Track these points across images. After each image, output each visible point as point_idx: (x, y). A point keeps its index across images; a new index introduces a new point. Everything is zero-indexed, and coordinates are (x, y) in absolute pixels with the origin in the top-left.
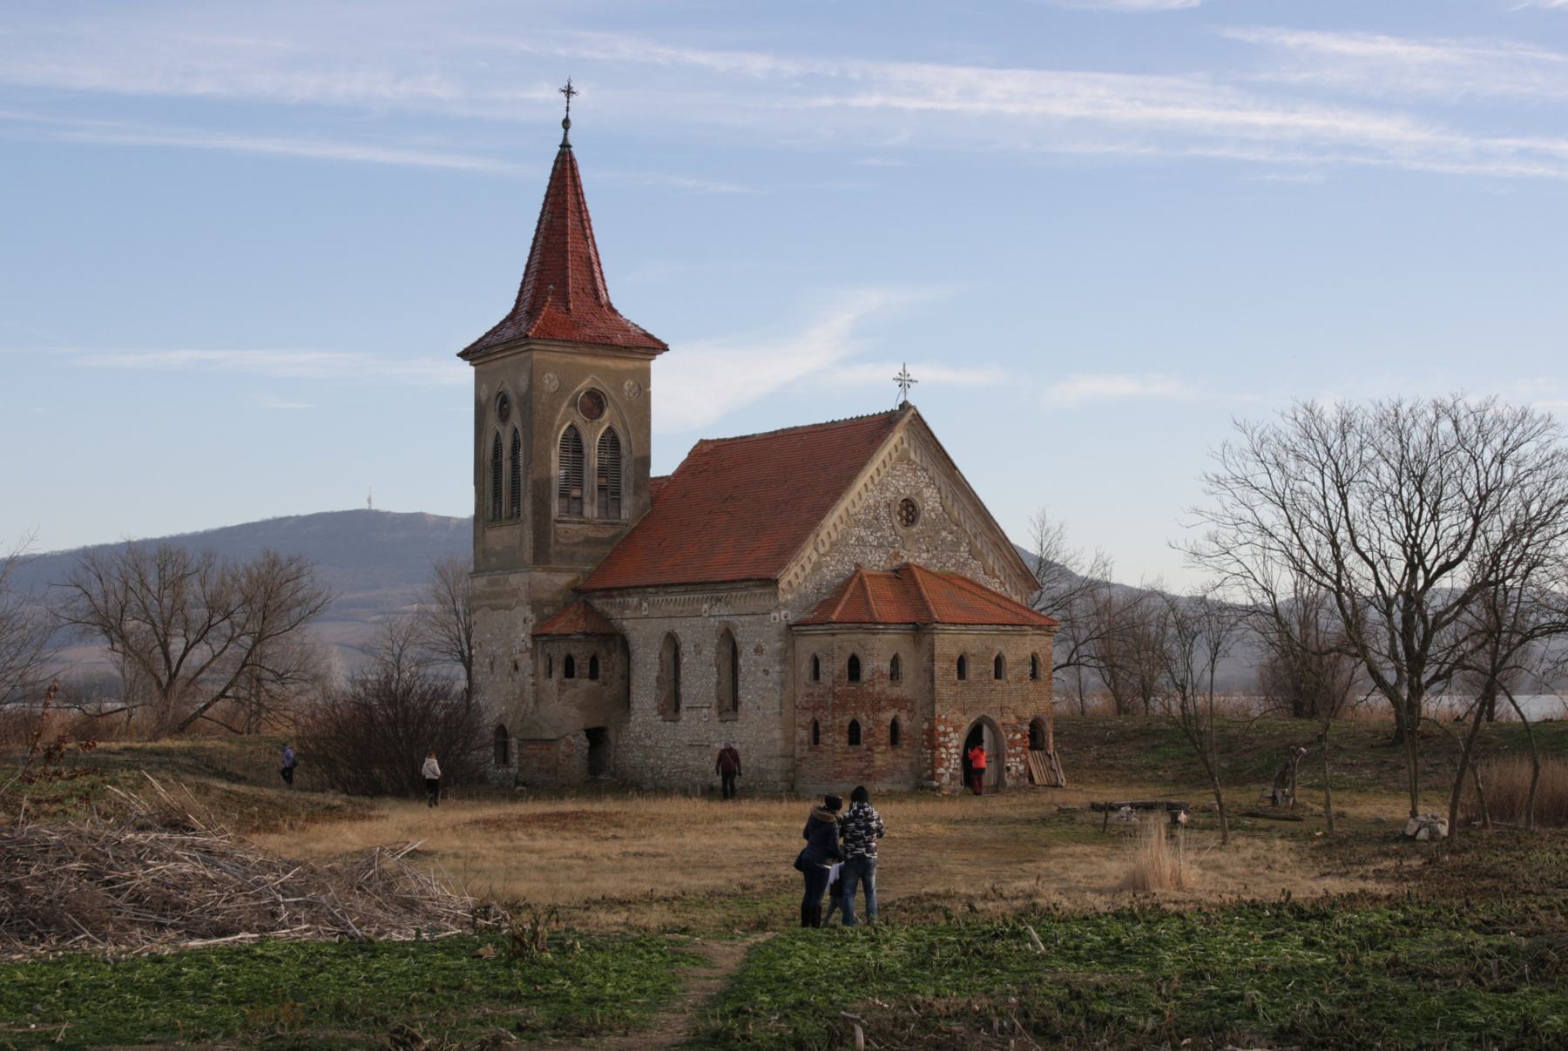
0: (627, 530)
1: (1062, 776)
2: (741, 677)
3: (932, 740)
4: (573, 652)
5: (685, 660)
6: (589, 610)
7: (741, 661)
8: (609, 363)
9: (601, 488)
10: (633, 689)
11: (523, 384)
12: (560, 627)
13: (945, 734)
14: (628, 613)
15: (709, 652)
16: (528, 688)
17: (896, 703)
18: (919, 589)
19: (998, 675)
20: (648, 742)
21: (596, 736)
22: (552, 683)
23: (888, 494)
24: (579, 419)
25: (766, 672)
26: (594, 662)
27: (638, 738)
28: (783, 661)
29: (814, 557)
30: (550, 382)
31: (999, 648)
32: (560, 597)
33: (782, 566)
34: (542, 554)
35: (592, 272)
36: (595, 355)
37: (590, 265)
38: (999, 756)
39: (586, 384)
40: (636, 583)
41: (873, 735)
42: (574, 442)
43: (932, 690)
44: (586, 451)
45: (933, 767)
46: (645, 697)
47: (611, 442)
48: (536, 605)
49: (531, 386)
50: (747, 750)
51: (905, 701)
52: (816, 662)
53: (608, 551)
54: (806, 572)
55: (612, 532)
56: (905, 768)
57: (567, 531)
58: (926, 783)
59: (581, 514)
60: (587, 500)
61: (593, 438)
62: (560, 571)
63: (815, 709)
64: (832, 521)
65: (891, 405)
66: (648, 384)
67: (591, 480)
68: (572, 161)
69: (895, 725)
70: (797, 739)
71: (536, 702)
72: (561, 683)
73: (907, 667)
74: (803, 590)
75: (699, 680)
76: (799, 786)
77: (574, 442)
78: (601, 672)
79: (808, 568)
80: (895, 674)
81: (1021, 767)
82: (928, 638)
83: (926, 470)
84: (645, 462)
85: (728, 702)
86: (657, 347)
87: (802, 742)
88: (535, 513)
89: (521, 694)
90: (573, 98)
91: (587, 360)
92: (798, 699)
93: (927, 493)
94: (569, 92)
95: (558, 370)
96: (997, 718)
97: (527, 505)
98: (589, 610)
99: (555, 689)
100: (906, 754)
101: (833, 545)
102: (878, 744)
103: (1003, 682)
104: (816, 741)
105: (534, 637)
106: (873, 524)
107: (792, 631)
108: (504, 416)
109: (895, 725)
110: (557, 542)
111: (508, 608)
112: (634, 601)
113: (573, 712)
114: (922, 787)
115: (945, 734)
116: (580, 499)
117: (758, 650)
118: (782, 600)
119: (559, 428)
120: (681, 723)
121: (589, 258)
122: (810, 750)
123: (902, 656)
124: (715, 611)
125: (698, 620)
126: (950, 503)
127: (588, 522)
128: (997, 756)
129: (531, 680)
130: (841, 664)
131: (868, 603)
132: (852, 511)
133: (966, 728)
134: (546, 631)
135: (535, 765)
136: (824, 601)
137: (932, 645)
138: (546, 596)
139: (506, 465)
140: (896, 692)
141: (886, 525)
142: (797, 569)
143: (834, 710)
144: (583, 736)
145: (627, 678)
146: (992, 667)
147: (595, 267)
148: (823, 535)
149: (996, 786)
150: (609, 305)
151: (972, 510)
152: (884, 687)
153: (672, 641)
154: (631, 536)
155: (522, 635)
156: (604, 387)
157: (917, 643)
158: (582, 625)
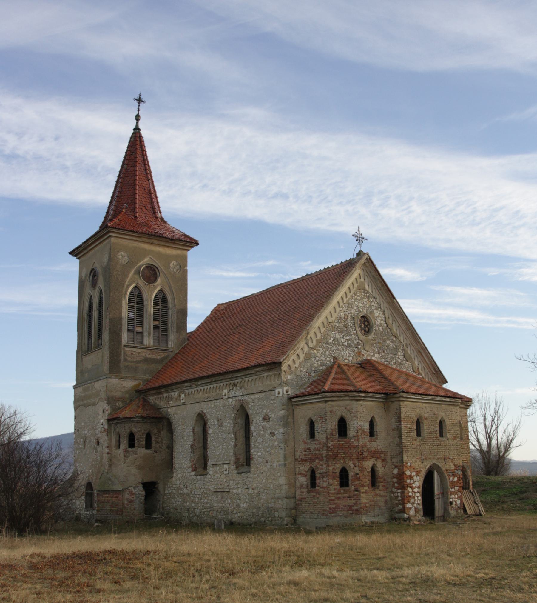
0: (172, 355)
1: (481, 508)
2: (252, 440)
3: (401, 481)
4: (134, 430)
5: (211, 431)
6: (146, 404)
7: (252, 428)
8: (161, 250)
9: (155, 327)
10: (175, 454)
11: (105, 259)
12: (126, 413)
13: (411, 477)
14: (172, 403)
15: (228, 424)
16: (106, 456)
17: (374, 454)
18: (381, 373)
20: (185, 491)
21: (150, 488)
22: (121, 451)
23: (353, 311)
24: (141, 283)
25: (273, 434)
26: (148, 438)
27: (179, 489)
28: (285, 425)
30: (122, 257)
31: (442, 414)
32: (127, 396)
33: (284, 353)
34: (115, 366)
35: (152, 198)
36: (152, 244)
37: (151, 195)
38: (444, 493)
39: (146, 260)
40: (174, 381)
41: (359, 479)
42: (137, 299)
43: (401, 443)
44: (145, 303)
45: (403, 504)
46: (183, 459)
47: (161, 300)
48: (111, 400)
49: (110, 259)
50: (258, 493)
51: (380, 452)
52: (312, 424)
53: (160, 368)
54: (301, 360)
55: (163, 355)
56: (382, 504)
57: (132, 353)
58: (397, 516)
59: (142, 343)
60: (146, 334)
61: (150, 295)
62: (126, 378)
63: (312, 460)
64: (318, 322)
65: (351, 255)
66: (186, 265)
67: (149, 321)
68: (141, 137)
69: (373, 471)
70: (298, 484)
71: (110, 466)
72: (126, 451)
73: (380, 427)
74: (298, 373)
75: (222, 444)
76: (300, 520)
77: (137, 299)
78: (154, 444)
79: (302, 357)
80: (372, 433)
81: (459, 502)
82: (394, 406)
83: (375, 298)
84: (183, 313)
85: (242, 459)
86: (190, 243)
87: (302, 486)
88: (111, 340)
89: (101, 461)
90: (142, 105)
91: (147, 246)
92: (298, 454)
93: (377, 313)
94: (139, 101)
95: (125, 248)
97: (106, 336)
98: (146, 404)
99: (122, 455)
100: (382, 493)
101: (318, 342)
102: (363, 486)
103: (444, 439)
104: (313, 483)
105: (109, 420)
106: (344, 330)
107: (292, 401)
108: (94, 284)
109: (373, 471)
110: (125, 360)
111: (94, 404)
112: (175, 394)
113: (134, 471)
114: (395, 519)
115: (411, 477)
116: (141, 333)
117: (266, 418)
118: (284, 377)
120: (208, 476)
121: (150, 190)
122: (308, 492)
123: (377, 418)
124: (232, 394)
125: (218, 404)
126: (390, 322)
127: (147, 348)
128: (443, 493)
129: (107, 450)
130: (333, 425)
131: (349, 379)
132: (330, 320)
133: (423, 473)
134: (116, 416)
135: (108, 508)
136: (314, 382)
137: (399, 410)
138: (118, 394)
139: (95, 314)
140: (373, 445)
141: (352, 332)
142: (294, 357)
143: (328, 460)
144: (141, 487)
145: (170, 448)
146: (438, 428)
147: (154, 200)
148: (311, 334)
149: (443, 516)
150: (162, 219)
151: (404, 327)
152: (365, 441)
153: (202, 419)
154: (174, 358)
155: (102, 420)
156: (157, 263)
157: (387, 409)
158: (140, 412)
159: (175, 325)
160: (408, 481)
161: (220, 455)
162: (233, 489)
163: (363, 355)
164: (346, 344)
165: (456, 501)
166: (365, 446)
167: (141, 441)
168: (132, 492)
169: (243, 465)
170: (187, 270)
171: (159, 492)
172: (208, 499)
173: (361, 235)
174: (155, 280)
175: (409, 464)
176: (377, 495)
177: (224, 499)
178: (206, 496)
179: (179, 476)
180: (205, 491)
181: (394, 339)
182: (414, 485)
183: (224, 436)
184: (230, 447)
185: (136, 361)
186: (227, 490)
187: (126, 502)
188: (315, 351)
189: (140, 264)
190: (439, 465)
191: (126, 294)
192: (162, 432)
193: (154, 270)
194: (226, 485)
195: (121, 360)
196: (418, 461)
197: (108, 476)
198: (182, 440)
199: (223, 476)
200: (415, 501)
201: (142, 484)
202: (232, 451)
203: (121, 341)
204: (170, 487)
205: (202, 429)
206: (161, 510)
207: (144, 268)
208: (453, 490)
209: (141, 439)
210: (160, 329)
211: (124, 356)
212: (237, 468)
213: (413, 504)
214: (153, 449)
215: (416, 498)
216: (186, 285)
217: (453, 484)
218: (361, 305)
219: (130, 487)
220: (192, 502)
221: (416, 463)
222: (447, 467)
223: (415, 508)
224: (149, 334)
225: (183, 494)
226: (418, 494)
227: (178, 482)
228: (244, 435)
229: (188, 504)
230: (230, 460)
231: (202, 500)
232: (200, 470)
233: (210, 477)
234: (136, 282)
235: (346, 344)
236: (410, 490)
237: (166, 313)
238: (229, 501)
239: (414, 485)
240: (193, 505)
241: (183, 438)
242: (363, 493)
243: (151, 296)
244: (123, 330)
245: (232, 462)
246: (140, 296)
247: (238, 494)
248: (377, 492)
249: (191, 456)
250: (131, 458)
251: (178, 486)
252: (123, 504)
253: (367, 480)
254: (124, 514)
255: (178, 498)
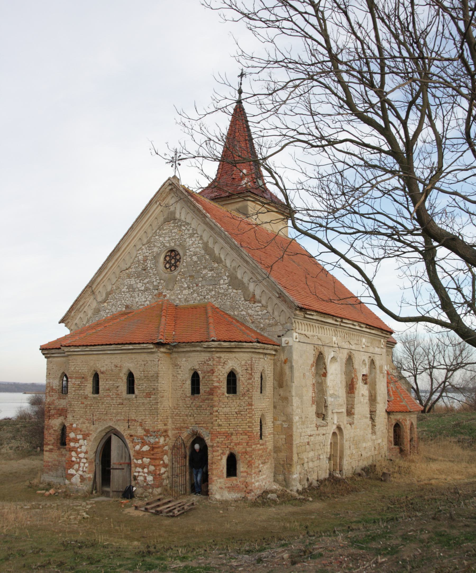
13: (76, 440)
19: (131, 390)
23: (155, 249)
29: (94, 305)
79: (90, 313)
96: (120, 428)
101: (108, 294)
115: (76, 440)
160: (72, 444)
163: (165, 296)
164: (143, 288)
165: (145, 477)
166: (53, 403)
173: (172, 158)
175: (74, 425)
176: (63, 455)
181: (216, 265)
182: (79, 450)
188: (106, 304)
190: (118, 428)
196: (87, 422)
200: (79, 467)
208: (140, 462)
213: (77, 470)
215: (82, 465)
217: (140, 455)
218: (167, 239)
221: (84, 425)
222: (132, 432)
223: (81, 476)
226: (84, 461)
235: (143, 288)
236: (73, 454)
239: (79, 450)
242: (46, 451)
248: (63, 452)
253: (51, 438)
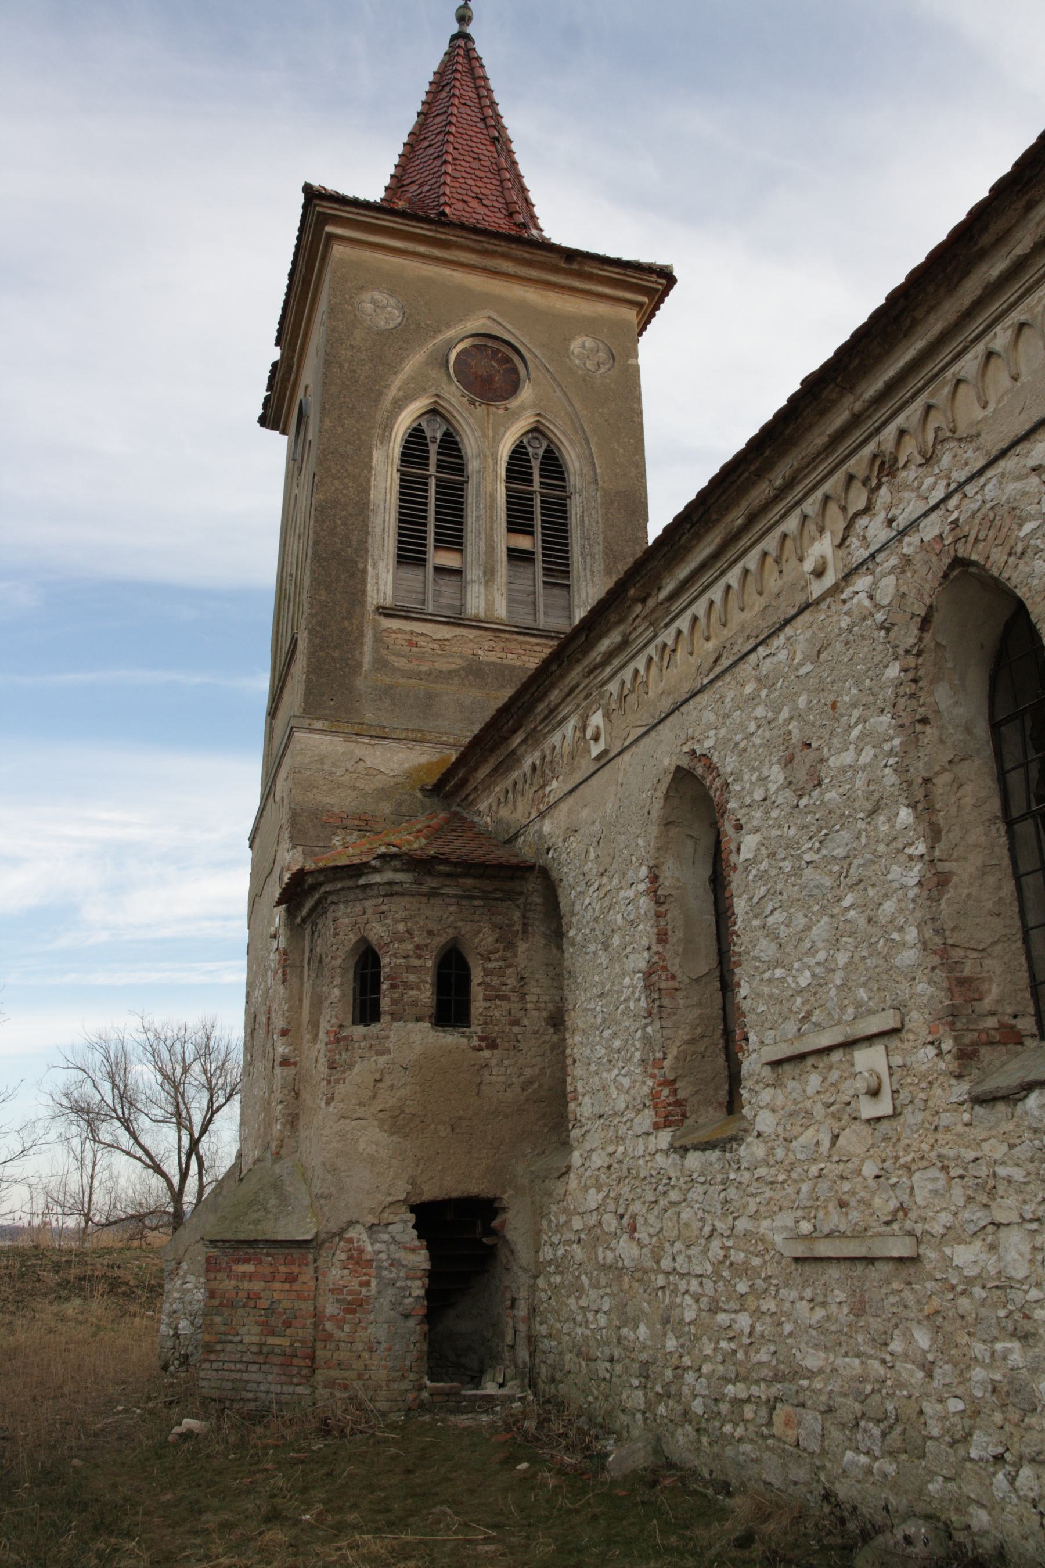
4: (377, 932)
8: (532, 295)
9: (516, 556)
20: (627, 1250)
24: (454, 396)
27: (595, 1237)
44: (473, 466)
46: (612, 1071)
60: (474, 574)
61: (490, 448)
72: (338, 1040)
78: (478, 1004)
86: (648, 286)
110: (381, 664)
113: (372, 1139)
119: (399, 405)
120: (752, 1150)
135: (251, 1335)
159: (598, 550)
161: (819, 983)
162: (951, 1235)
167: (408, 986)
168: (361, 1251)
169: (1011, 1037)
170: (636, 369)
171: (512, 1252)
172: (758, 1314)
174: (513, 388)
177: (876, 1324)
178: (742, 1287)
179: (598, 1160)
180: (738, 1257)
183: (840, 844)
184: (889, 907)
185: (429, 674)
186: (900, 1248)
187: (331, 1309)
189: (451, 333)
191: (388, 426)
192: (522, 946)
193: (508, 360)
194: (884, 1204)
195: (360, 665)
197: (277, 1168)
198: (603, 959)
199: (853, 1140)
201: (413, 1209)
202: (912, 934)
203: (364, 593)
204: (559, 1229)
205: (706, 873)
206: (523, 1354)
207: (464, 351)
209: (412, 978)
210: (539, 565)
211: (375, 650)
212: (966, 1055)
214: (476, 1028)
216: (640, 414)
219: (351, 1223)
220: (666, 1321)
224: (490, 574)
225: (615, 1269)
227: (594, 1198)
228: (995, 805)
229: (643, 1330)
230: (898, 1008)
231: (722, 1318)
232: (708, 1120)
233: (759, 1150)
234: (433, 390)
237: (557, 513)
238: (923, 1339)
240: (671, 1344)
241: (606, 947)
243: (496, 441)
244: (374, 550)
245: (916, 1020)
246: (451, 444)
247: (1005, 1284)
249: (647, 1039)
250: (360, 1073)
251: (592, 1220)
252: (318, 1317)
254: (320, 1376)
255: (593, 1294)
